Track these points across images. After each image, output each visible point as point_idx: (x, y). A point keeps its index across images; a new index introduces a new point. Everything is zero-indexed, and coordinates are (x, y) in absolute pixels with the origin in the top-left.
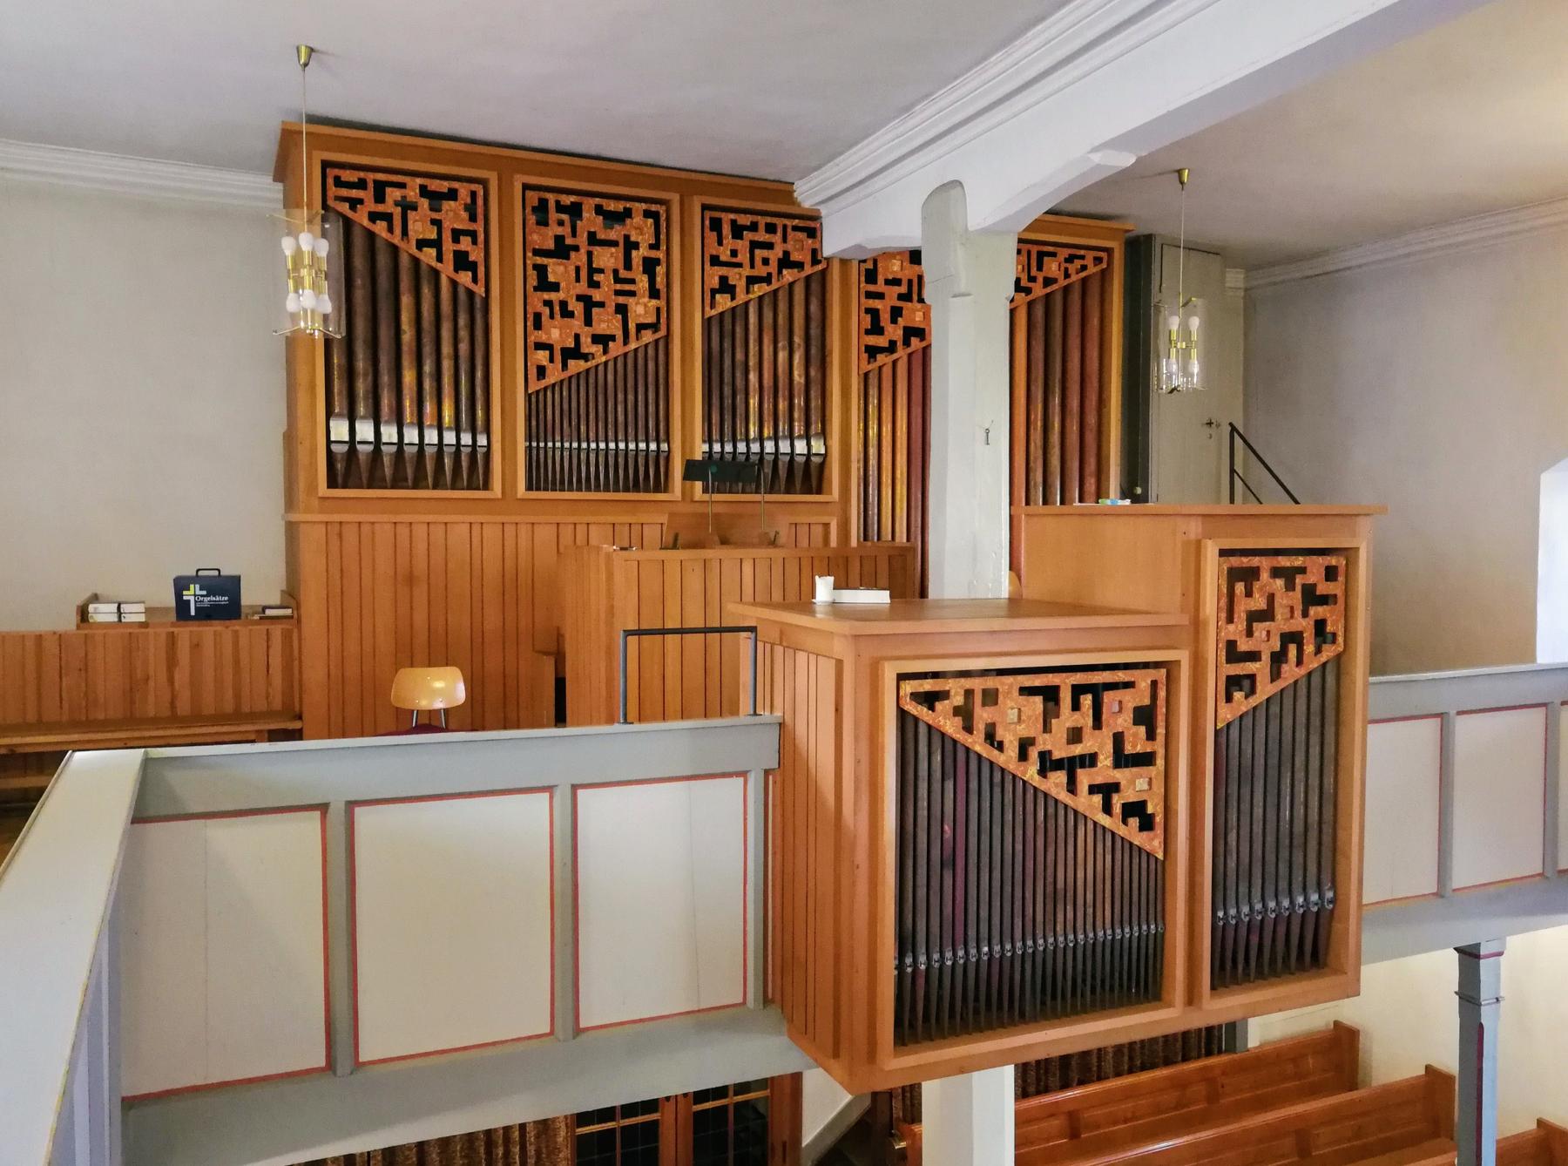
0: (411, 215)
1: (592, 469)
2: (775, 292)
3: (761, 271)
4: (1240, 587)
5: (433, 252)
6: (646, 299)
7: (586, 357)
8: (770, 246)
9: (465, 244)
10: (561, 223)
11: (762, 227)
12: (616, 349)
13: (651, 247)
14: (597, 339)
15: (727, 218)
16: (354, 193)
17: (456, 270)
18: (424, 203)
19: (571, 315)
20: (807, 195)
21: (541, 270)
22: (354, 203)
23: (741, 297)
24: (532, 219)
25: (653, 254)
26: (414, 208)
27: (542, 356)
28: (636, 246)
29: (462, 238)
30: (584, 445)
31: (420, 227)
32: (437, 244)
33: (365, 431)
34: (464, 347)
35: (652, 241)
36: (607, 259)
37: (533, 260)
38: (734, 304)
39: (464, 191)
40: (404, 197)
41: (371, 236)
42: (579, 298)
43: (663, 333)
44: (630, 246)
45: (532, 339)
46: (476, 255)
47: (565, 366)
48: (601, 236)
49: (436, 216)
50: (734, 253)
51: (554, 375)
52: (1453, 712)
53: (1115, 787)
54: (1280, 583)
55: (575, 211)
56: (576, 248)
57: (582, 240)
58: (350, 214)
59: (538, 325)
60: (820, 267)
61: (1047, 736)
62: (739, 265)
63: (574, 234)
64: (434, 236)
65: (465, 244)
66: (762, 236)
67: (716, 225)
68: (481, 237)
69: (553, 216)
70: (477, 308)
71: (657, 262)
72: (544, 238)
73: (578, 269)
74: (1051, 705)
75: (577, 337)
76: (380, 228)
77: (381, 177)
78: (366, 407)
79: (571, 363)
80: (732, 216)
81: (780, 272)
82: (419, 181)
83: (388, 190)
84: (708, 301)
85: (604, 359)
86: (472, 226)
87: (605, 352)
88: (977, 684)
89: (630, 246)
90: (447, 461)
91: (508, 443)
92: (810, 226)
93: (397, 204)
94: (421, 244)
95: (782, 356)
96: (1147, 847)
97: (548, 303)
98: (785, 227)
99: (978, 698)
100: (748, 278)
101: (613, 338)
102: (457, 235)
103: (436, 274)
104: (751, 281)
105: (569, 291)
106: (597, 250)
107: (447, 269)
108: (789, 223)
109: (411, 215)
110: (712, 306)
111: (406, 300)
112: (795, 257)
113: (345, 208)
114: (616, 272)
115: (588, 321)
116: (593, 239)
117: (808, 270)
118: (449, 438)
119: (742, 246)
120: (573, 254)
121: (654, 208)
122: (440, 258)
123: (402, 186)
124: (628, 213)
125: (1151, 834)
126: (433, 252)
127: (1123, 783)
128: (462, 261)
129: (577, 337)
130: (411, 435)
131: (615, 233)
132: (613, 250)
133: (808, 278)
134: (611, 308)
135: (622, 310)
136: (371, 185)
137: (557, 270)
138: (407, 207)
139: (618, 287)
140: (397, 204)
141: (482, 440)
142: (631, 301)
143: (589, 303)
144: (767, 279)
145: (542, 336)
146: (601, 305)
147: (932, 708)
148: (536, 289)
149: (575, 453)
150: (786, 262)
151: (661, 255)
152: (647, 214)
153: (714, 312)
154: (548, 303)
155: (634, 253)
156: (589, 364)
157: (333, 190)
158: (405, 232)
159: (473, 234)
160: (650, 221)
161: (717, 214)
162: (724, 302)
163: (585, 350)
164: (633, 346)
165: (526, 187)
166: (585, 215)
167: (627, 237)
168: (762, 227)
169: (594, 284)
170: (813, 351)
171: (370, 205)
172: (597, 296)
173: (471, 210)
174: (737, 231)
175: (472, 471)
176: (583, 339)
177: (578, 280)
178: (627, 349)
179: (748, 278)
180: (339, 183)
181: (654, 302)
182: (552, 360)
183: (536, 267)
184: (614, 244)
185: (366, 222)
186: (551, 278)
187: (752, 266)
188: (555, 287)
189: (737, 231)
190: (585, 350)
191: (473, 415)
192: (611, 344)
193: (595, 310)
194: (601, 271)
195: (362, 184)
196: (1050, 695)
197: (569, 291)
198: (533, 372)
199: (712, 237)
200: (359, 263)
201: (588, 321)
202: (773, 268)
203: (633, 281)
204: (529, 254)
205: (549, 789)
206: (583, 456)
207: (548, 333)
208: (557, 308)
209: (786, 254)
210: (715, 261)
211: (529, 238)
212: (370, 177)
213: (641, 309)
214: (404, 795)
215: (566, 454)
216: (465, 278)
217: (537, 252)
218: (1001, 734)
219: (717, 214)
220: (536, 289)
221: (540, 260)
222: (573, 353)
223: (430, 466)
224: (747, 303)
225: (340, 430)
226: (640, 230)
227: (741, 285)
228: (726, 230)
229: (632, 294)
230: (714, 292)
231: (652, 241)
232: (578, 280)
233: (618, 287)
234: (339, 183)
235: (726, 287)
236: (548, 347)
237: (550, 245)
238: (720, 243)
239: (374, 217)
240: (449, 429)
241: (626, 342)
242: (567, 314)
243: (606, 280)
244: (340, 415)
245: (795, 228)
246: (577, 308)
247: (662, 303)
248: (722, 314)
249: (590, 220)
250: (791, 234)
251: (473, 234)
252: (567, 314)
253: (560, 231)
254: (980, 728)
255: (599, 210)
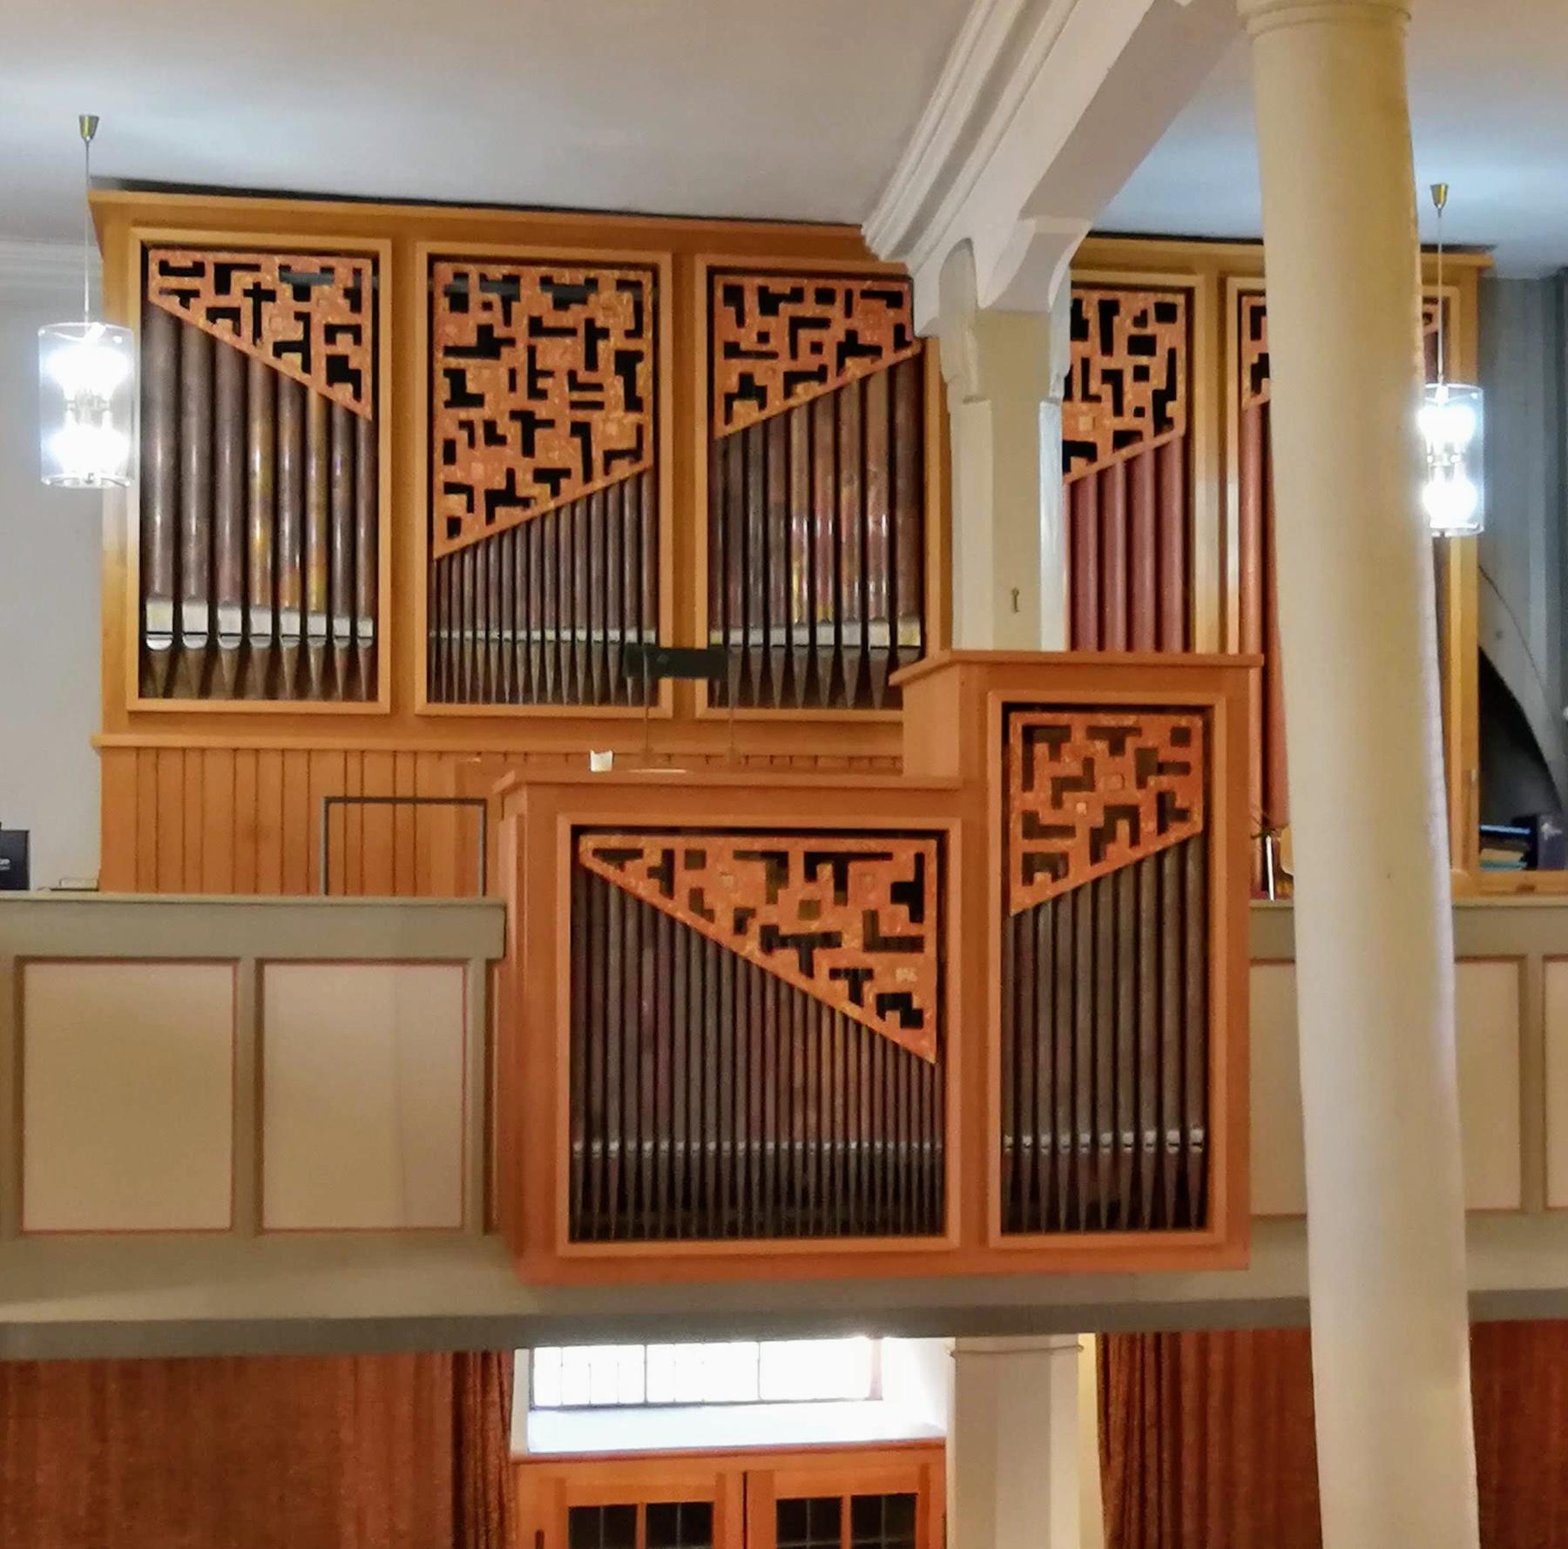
0: (267, 307)
1: (535, 672)
2: (837, 393)
3: (808, 362)
4: (1041, 749)
5: (297, 358)
6: (620, 413)
7: (525, 502)
8: (823, 323)
9: (344, 344)
10: (487, 306)
11: (810, 296)
12: (572, 488)
13: (629, 334)
14: (541, 475)
15: (751, 285)
16: (188, 283)
17: (331, 380)
18: (285, 291)
19: (502, 440)
20: (882, 239)
21: (457, 377)
22: (186, 296)
23: (776, 404)
24: (443, 303)
25: (632, 345)
26: (271, 296)
27: (456, 503)
28: (605, 333)
29: (339, 337)
30: (522, 635)
31: (280, 322)
32: (303, 347)
33: (196, 617)
34: (340, 494)
35: (631, 326)
36: (560, 355)
37: (444, 362)
38: (765, 414)
39: (343, 268)
40: (257, 285)
41: (211, 343)
42: (515, 415)
43: (647, 460)
44: (595, 333)
45: (440, 479)
46: (359, 359)
47: (490, 517)
48: (550, 320)
49: (303, 307)
50: (763, 337)
51: (475, 529)
52: (1534, 956)
53: (869, 974)
54: (1101, 746)
55: (510, 289)
56: (511, 342)
57: (520, 328)
58: (180, 312)
59: (450, 456)
60: (908, 353)
61: (771, 907)
62: (773, 355)
63: (507, 320)
64: (297, 334)
65: (344, 344)
66: (809, 309)
67: (734, 296)
68: (367, 334)
69: (476, 297)
70: (354, 434)
71: (638, 356)
72: (460, 329)
73: (513, 373)
74: (841, 894)
75: (511, 474)
76: (222, 329)
77: (225, 257)
78: (263, 596)
79: (501, 512)
80: (760, 281)
81: (841, 365)
82: (278, 260)
83: (235, 275)
84: (1247, 383)
85: (552, 505)
86: (353, 319)
87: (555, 492)
88: (679, 844)
89: (595, 333)
90: (314, 661)
91: (402, 631)
92: (893, 291)
93: (247, 293)
94: (280, 348)
95: (848, 493)
96: (912, 1047)
97: (467, 425)
98: (849, 294)
99: (679, 860)
100: (786, 374)
101: (566, 473)
102: (331, 332)
103: (302, 390)
104: (792, 379)
105: (499, 404)
106: (542, 343)
107: (317, 382)
108: (857, 286)
109: (267, 307)
110: (728, 419)
111: (258, 429)
112: (866, 338)
113: (173, 304)
114: (572, 375)
115: (528, 449)
116: (536, 327)
117: (889, 357)
118: (317, 625)
119: (777, 326)
120: (505, 351)
121: (632, 276)
122: (306, 367)
123: (255, 268)
124: (592, 284)
125: (917, 1032)
126: (297, 358)
127: (877, 970)
128: (339, 370)
129: (511, 474)
130: (261, 622)
131: (573, 317)
132: (568, 341)
133: (892, 371)
134: (564, 428)
135: (581, 430)
136: (210, 271)
137: (481, 375)
138: (260, 295)
139: (576, 396)
140: (247, 293)
141: (365, 628)
142: (595, 417)
143: (529, 422)
144: (821, 375)
145: (456, 474)
146: (550, 423)
147: (621, 867)
148: (448, 404)
149: (507, 647)
150: (851, 347)
151: (644, 345)
152: (622, 285)
153: (730, 429)
154: (467, 425)
155: (601, 345)
156: (529, 513)
157: (156, 281)
158: (257, 333)
159: (356, 331)
160: (627, 296)
161: (733, 280)
162: (747, 413)
163: (522, 492)
164: (599, 483)
165: (433, 259)
166: (525, 292)
167: (590, 323)
168: (810, 296)
169: (536, 393)
170: (901, 483)
171: (210, 298)
172: (542, 410)
173: (354, 296)
174: (769, 304)
175: (349, 672)
176: (519, 476)
177: (513, 387)
178: (589, 488)
179: (786, 374)
180: (165, 269)
181: (633, 417)
182: (470, 508)
183: (448, 372)
184: (571, 332)
185: (202, 322)
186: (471, 388)
187: (794, 354)
188: (478, 400)
189: (769, 304)
190: (522, 492)
191: (347, 592)
192: (564, 483)
193: (539, 434)
194: (549, 374)
195: (197, 270)
196: (779, 861)
197: (499, 404)
198: (441, 527)
199: (726, 314)
200: (194, 380)
201: (528, 449)
202: (829, 357)
203: (598, 387)
204: (439, 355)
205: (232, 961)
206: (520, 651)
207: (468, 471)
208: (480, 432)
209: (852, 335)
210: (733, 350)
211: (438, 331)
212: (210, 259)
213: (613, 427)
214: (74, 954)
215: (494, 648)
216: (342, 393)
217: (450, 351)
218: (709, 900)
219: (733, 280)
220: (448, 404)
221: (454, 362)
222: (505, 496)
223: (288, 667)
224: (788, 414)
225: (160, 615)
226: (611, 309)
227: (775, 388)
228: (751, 302)
229: (599, 405)
230: (730, 398)
231: (631, 326)
232: (513, 387)
233: (576, 396)
234: (165, 269)
235: (749, 389)
236: (467, 490)
237: (471, 339)
238: (740, 322)
239: (214, 314)
240: (317, 612)
241: (588, 476)
242: (493, 437)
243: (556, 388)
244: (160, 597)
245: (866, 294)
246: (511, 430)
247: (646, 418)
248: (746, 431)
249: (534, 300)
250: (859, 304)
251: (356, 331)
252: (493, 437)
253: (485, 318)
254: (682, 894)
255: (546, 282)
